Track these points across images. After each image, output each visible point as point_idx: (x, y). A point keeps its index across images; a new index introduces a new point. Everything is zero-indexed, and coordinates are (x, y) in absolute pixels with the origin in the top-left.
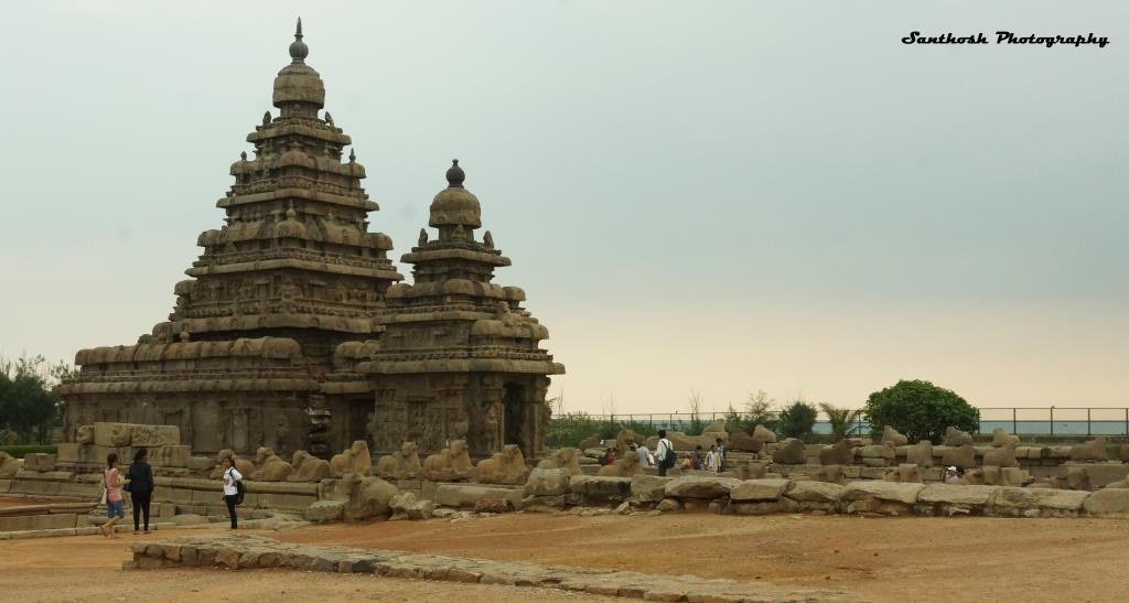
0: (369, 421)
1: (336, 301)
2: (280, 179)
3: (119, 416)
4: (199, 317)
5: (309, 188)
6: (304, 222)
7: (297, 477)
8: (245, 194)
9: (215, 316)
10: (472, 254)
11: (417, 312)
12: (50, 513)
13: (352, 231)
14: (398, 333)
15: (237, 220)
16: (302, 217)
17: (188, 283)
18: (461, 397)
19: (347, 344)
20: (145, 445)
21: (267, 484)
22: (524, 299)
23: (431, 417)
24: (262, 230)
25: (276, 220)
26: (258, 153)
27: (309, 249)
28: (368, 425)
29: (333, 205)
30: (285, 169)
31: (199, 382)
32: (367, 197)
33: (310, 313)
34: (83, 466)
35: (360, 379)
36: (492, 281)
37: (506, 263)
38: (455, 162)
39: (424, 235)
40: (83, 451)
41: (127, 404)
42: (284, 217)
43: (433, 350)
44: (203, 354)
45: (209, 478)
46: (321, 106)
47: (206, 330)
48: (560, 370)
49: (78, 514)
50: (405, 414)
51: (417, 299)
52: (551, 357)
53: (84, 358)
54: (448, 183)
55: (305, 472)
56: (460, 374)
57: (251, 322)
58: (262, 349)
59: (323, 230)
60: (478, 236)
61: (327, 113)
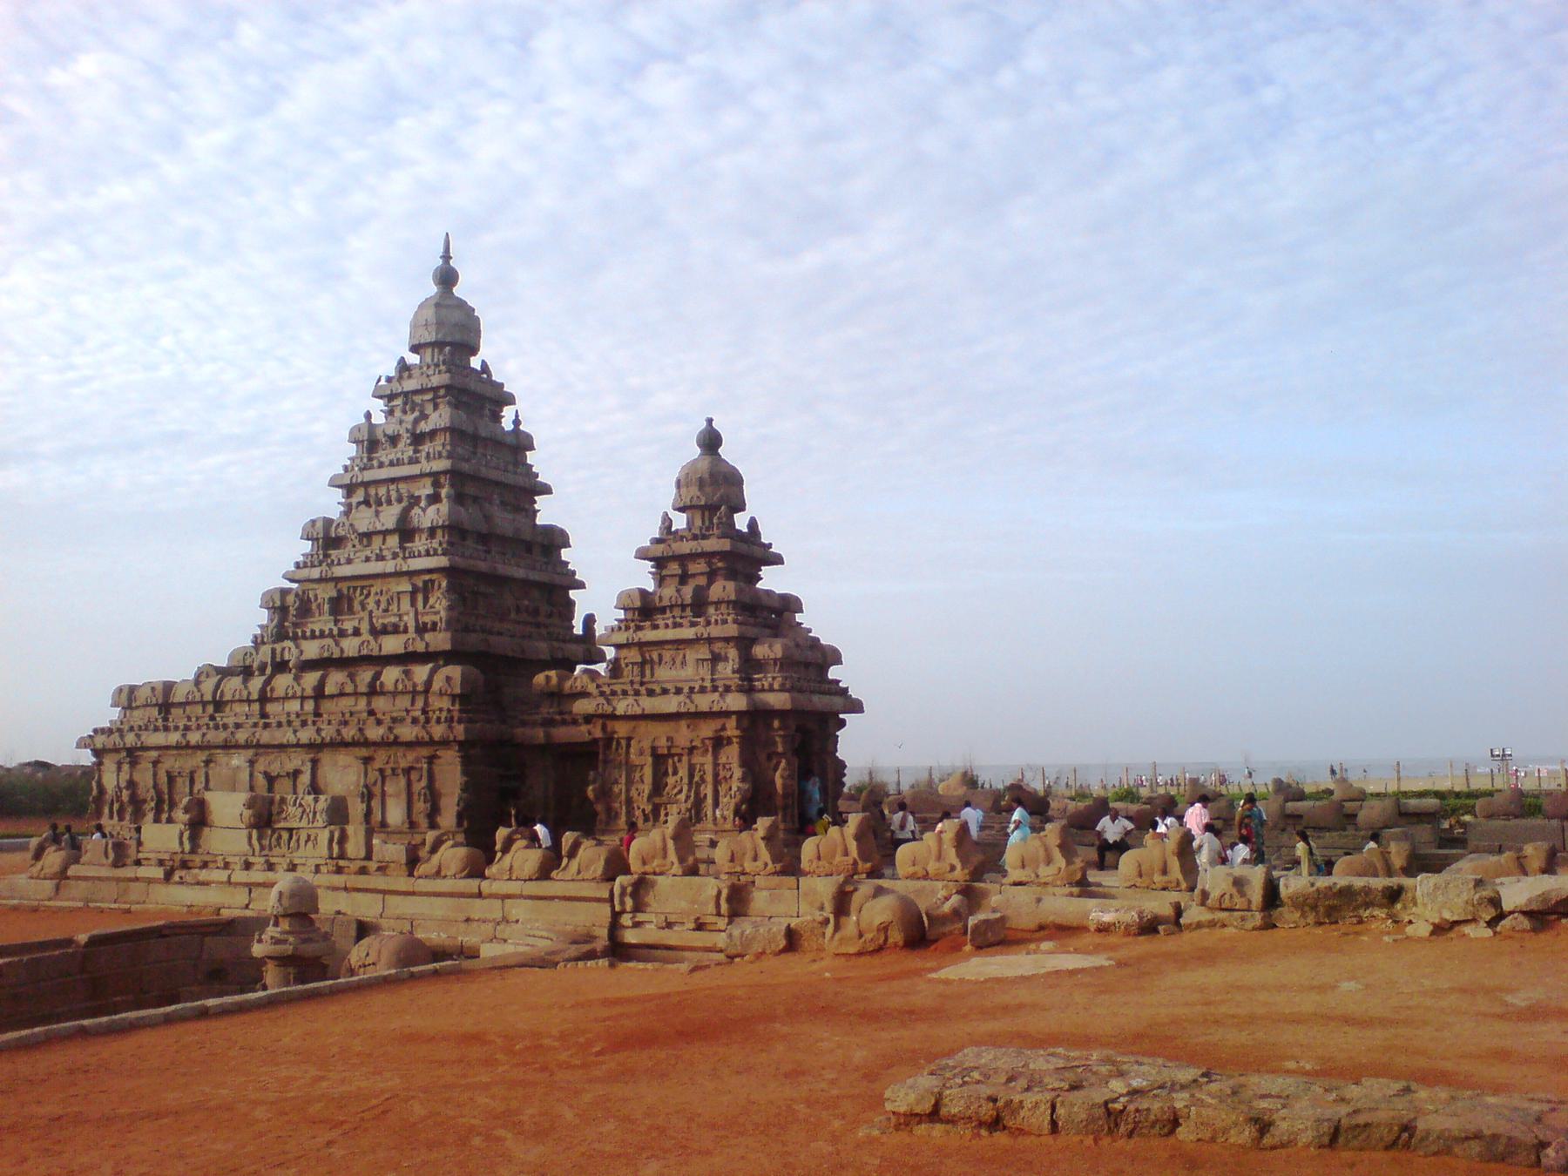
1: (503, 617)
2: (426, 448)
5: (468, 460)
6: (462, 505)
8: (372, 467)
9: (331, 635)
10: (743, 548)
11: (667, 626)
15: (359, 504)
17: (284, 592)
19: (552, 673)
20: (295, 825)
22: (802, 612)
23: (691, 776)
24: (404, 517)
25: (423, 504)
27: (469, 542)
29: (498, 484)
30: (433, 434)
32: (537, 475)
33: (474, 631)
34: (187, 857)
36: (759, 585)
37: (777, 560)
38: (710, 421)
39: (667, 522)
40: (186, 835)
42: (434, 499)
45: (411, 874)
46: (474, 350)
47: (319, 657)
48: (857, 707)
49: (205, 935)
51: (663, 610)
52: (846, 690)
53: (128, 698)
54: (698, 451)
57: (391, 645)
58: (429, 683)
59: (488, 518)
60: (741, 522)
61: (483, 362)
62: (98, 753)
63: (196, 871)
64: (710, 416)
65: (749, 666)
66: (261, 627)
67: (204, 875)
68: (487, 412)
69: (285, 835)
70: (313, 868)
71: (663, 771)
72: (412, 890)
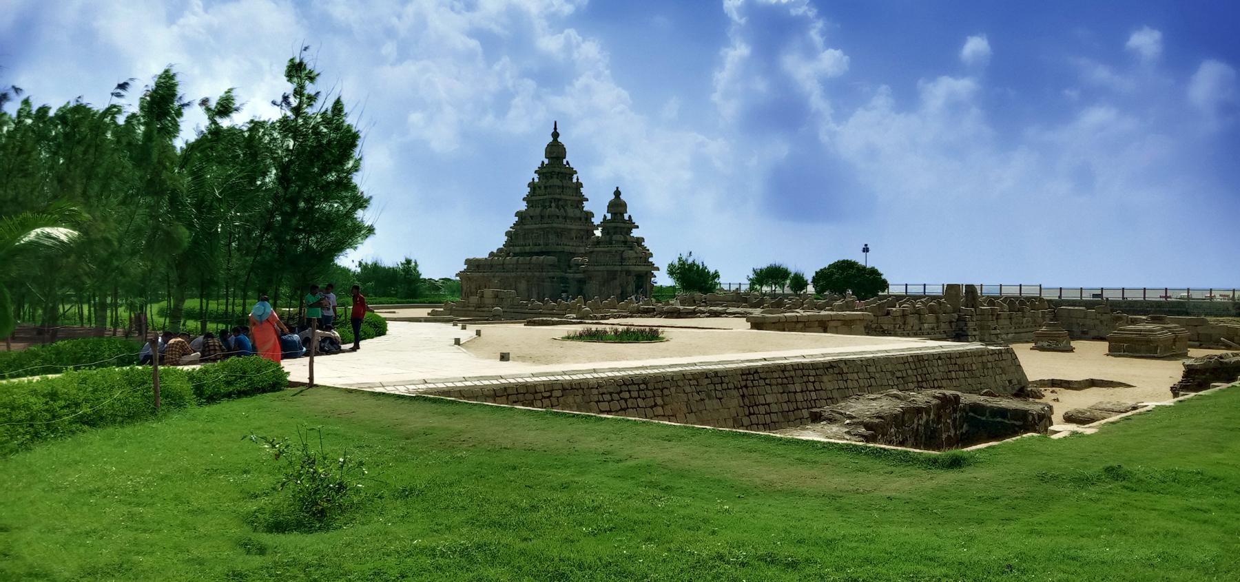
10: (622, 225)
13: (577, 212)
16: (557, 207)
26: (539, 179)
36: (632, 235)
37: (637, 227)
38: (617, 188)
42: (550, 207)
44: (520, 262)
46: (565, 158)
52: (654, 264)
53: (468, 262)
57: (537, 249)
58: (543, 262)
60: (626, 217)
61: (567, 162)
64: (617, 186)
65: (622, 259)
67: (483, 309)
68: (567, 178)
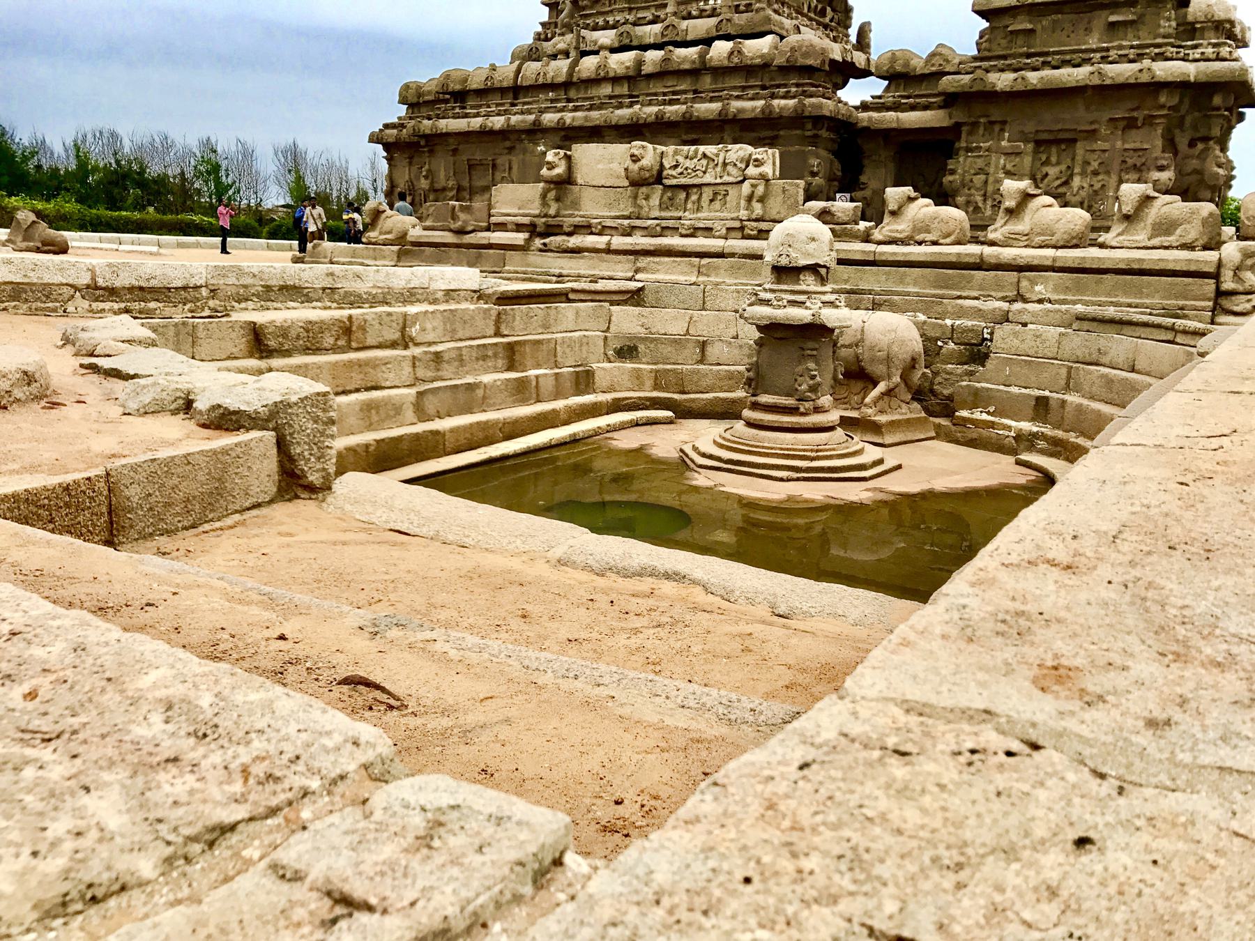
0: (953, 172)
3: (494, 166)
4: (596, 28)
7: (1141, 237)
12: (569, 301)
14: (1023, 24)
18: (1159, 131)
21: (1050, 252)
28: (948, 179)
31: (654, 109)
35: (926, 108)
40: (552, 195)
41: (511, 149)
43: (1107, 50)
44: (647, 69)
49: (612, 303)
50: (1028, 160)
55: (1166, 227)
56: (1182, 86)
62: (387, 147)
63: (565, 238)
66: (543, 24)
67: (574, 241)
69: (683, 195)
70: (724, 231)
71: (1044, 158)
72: (871, 258)
